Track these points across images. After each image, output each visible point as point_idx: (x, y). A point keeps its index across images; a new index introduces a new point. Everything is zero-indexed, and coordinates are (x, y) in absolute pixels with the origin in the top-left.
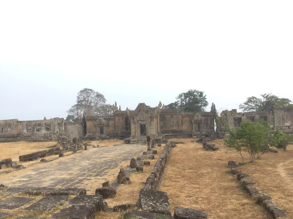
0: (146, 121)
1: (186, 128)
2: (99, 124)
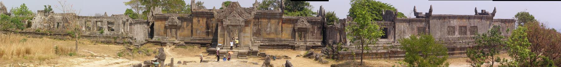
1: (287, 37)
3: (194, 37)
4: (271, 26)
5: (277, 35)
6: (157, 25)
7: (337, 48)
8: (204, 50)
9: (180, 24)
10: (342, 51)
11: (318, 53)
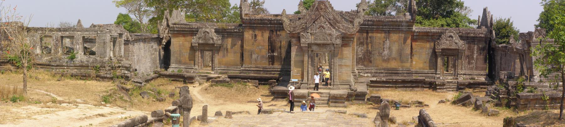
0: (331, 46)
1: (421, 65)
2: (202, 44)
3: (246, 66)
4: (390, 46)
5: (402, 62)
6: (177, 43)
7: (515, 87)
8: (265, 90)
9: (219, 42)
10: (524, 93)
11: (480, 95)
